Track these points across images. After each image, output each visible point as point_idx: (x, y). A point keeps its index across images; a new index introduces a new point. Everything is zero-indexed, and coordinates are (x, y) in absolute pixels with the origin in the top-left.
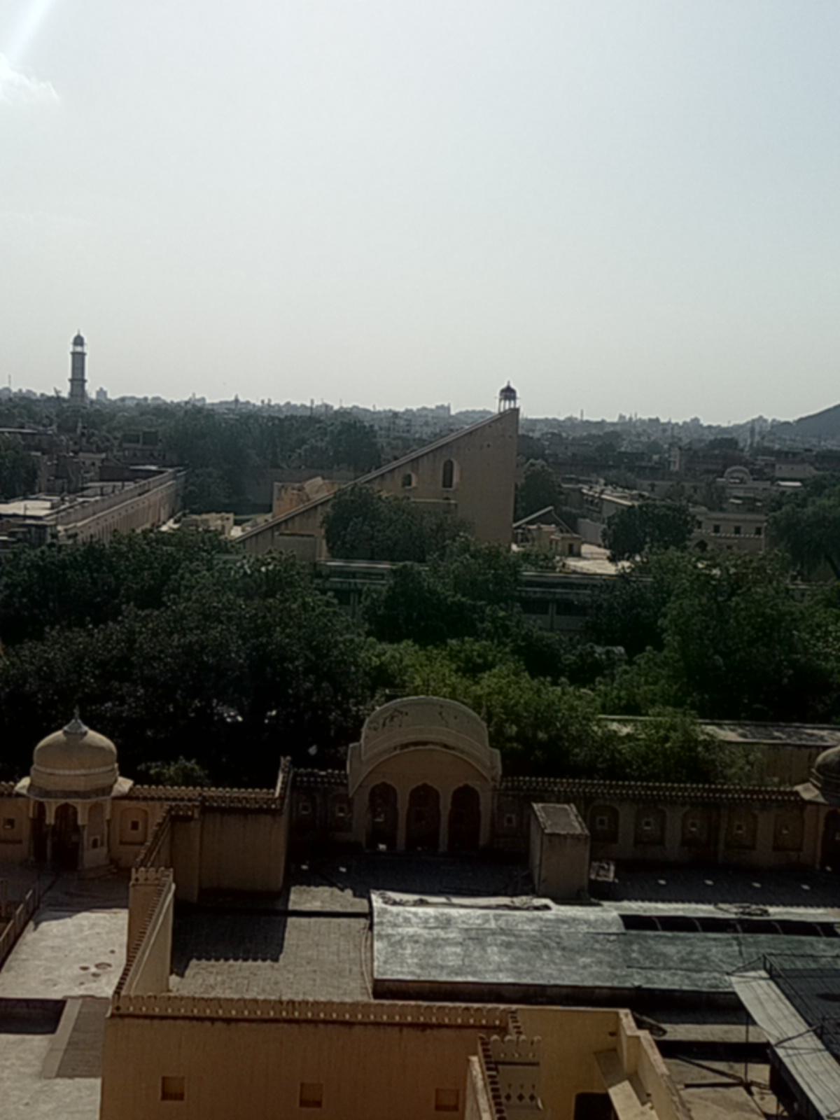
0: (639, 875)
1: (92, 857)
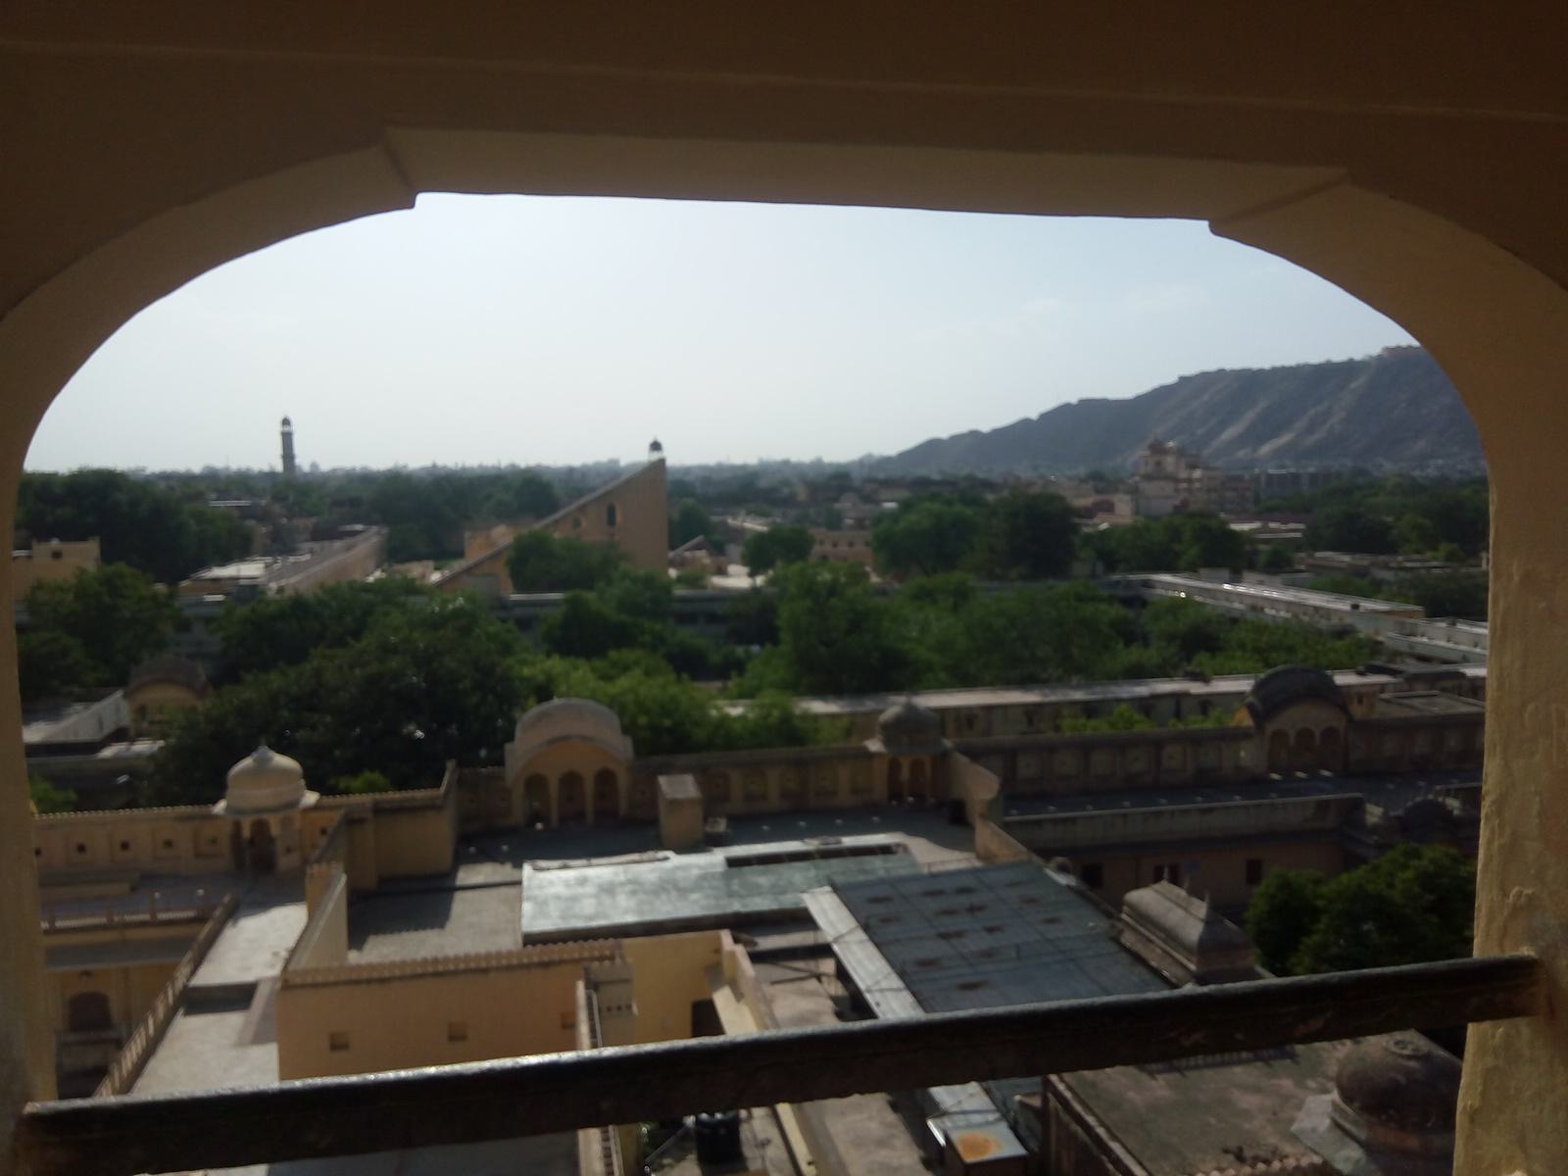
0: (746, 826)
1: (285, 862)
